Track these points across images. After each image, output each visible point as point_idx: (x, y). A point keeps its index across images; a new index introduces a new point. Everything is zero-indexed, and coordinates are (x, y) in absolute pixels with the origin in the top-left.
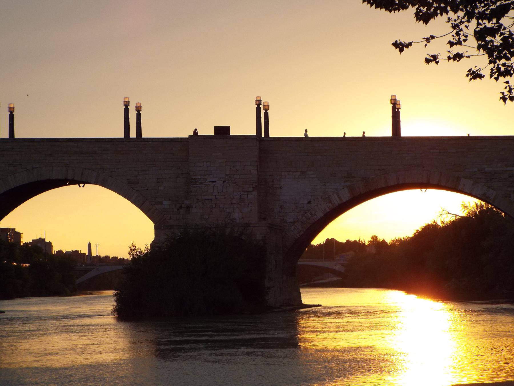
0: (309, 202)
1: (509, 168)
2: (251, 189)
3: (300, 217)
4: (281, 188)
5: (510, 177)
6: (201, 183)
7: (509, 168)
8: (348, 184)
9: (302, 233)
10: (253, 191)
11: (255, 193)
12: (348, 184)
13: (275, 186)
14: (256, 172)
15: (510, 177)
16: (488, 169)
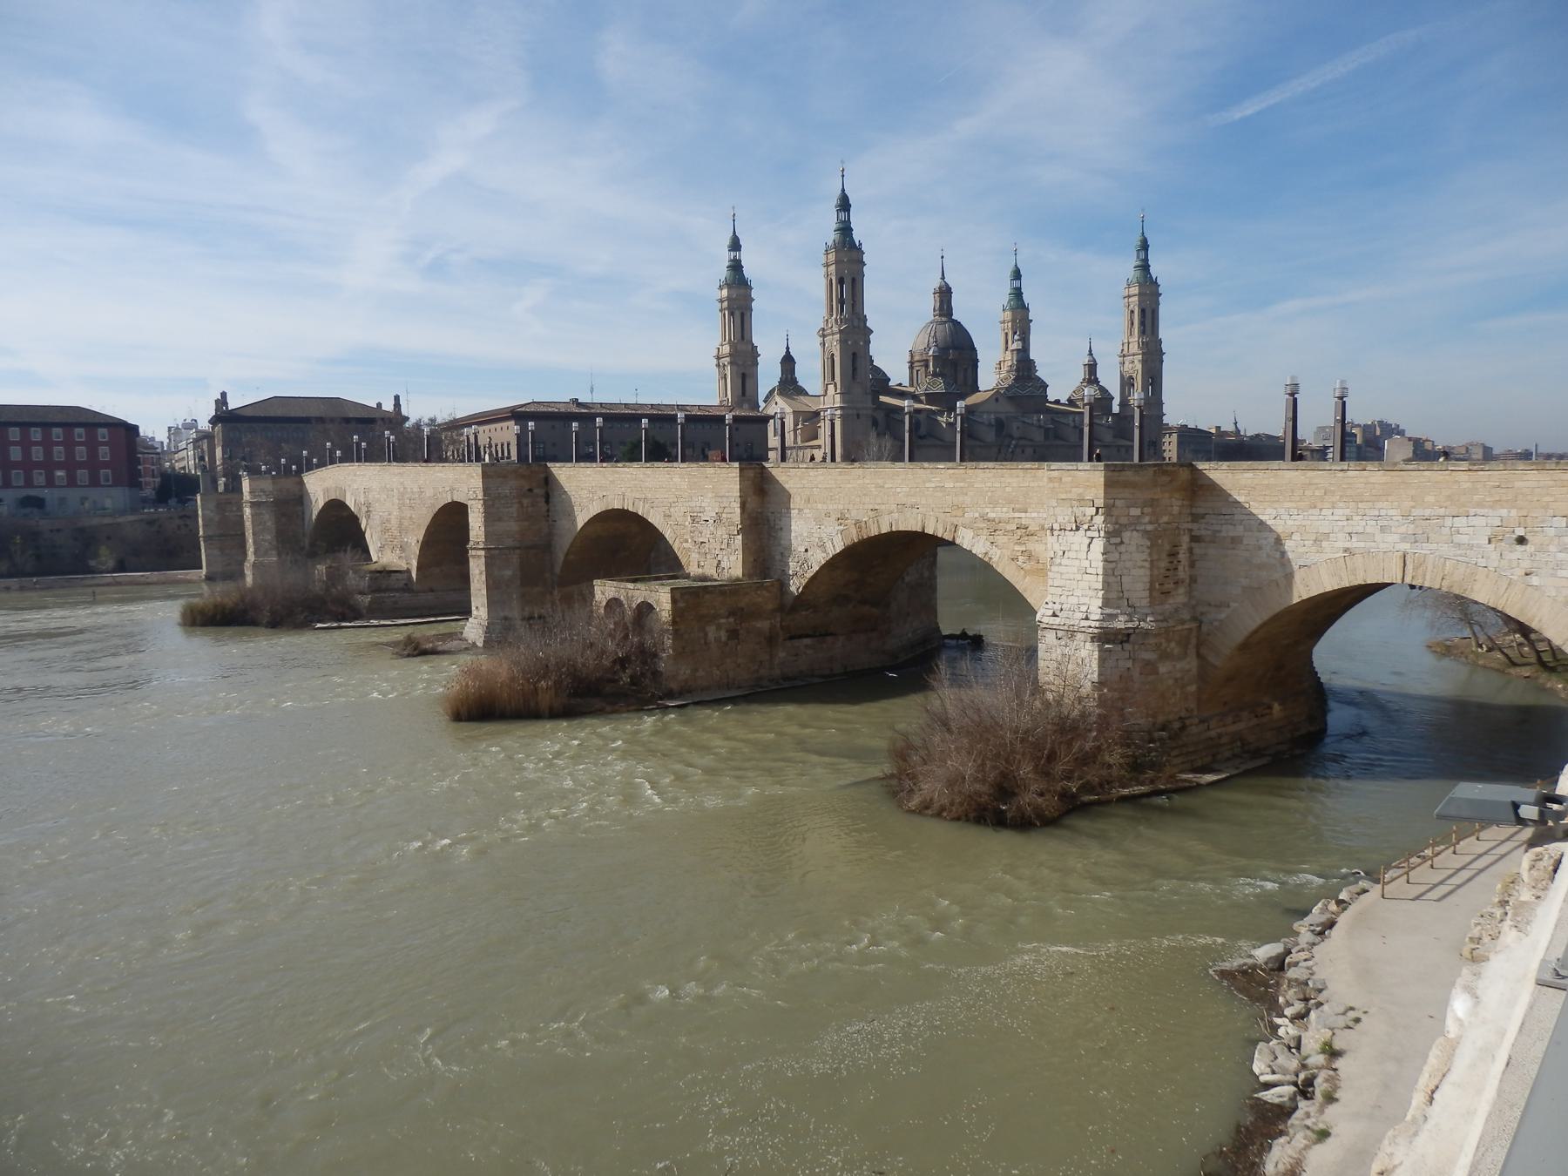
0: (806, 550)
1: (1017, 515)
2: (736, 533)
3: (798, 569)
4: (781, 529)
5: (1018, 528)
6: (698, 523)
7: (1017, 515)
8: (842, 528)
9: (800, 590)
10: (738, 534)
11: (740, 537)
12: (842, 528)
13: (777, 527)
14: (738, 511)
15: (1018, 528)
16: (991, 515)
